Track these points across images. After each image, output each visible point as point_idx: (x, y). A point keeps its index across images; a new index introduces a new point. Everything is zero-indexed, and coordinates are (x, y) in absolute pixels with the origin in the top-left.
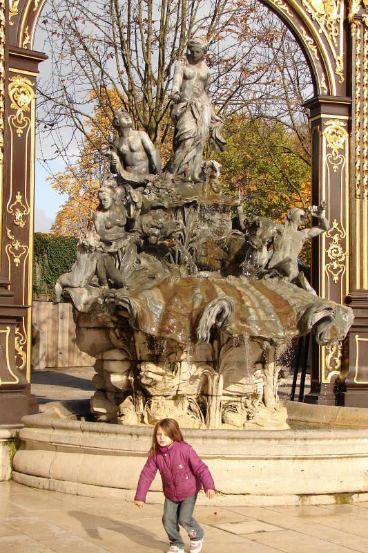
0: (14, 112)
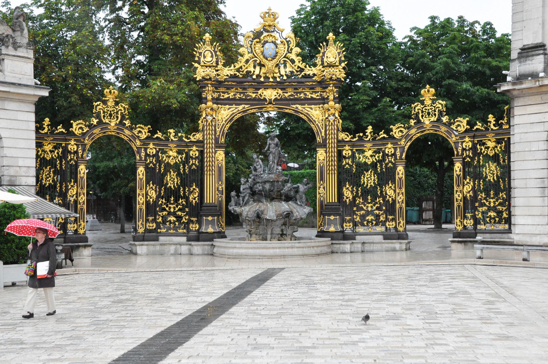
0: (218, 160)
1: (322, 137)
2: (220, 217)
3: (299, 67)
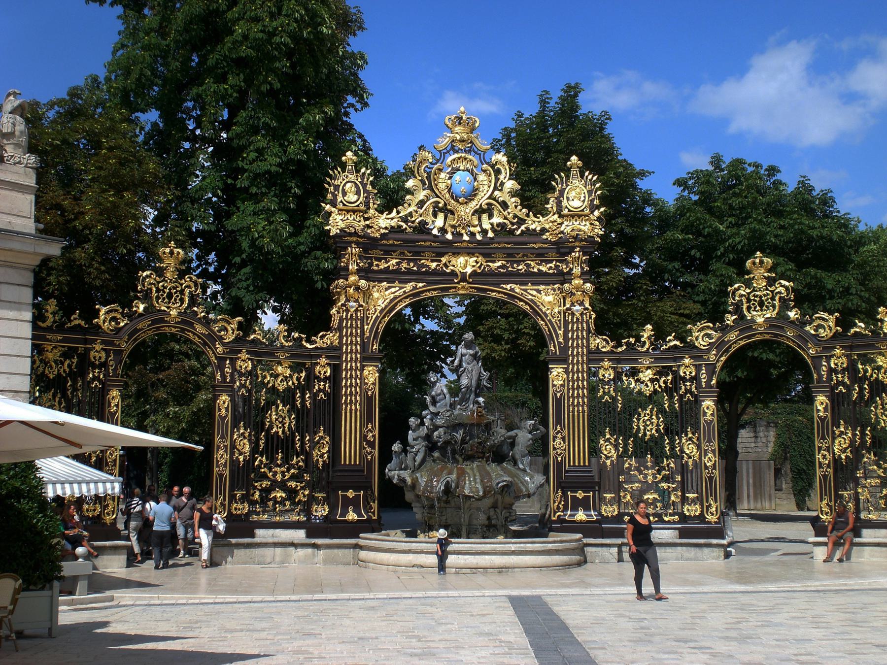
1: (559, 343)
2: (369, 492)
3: (515, 216)
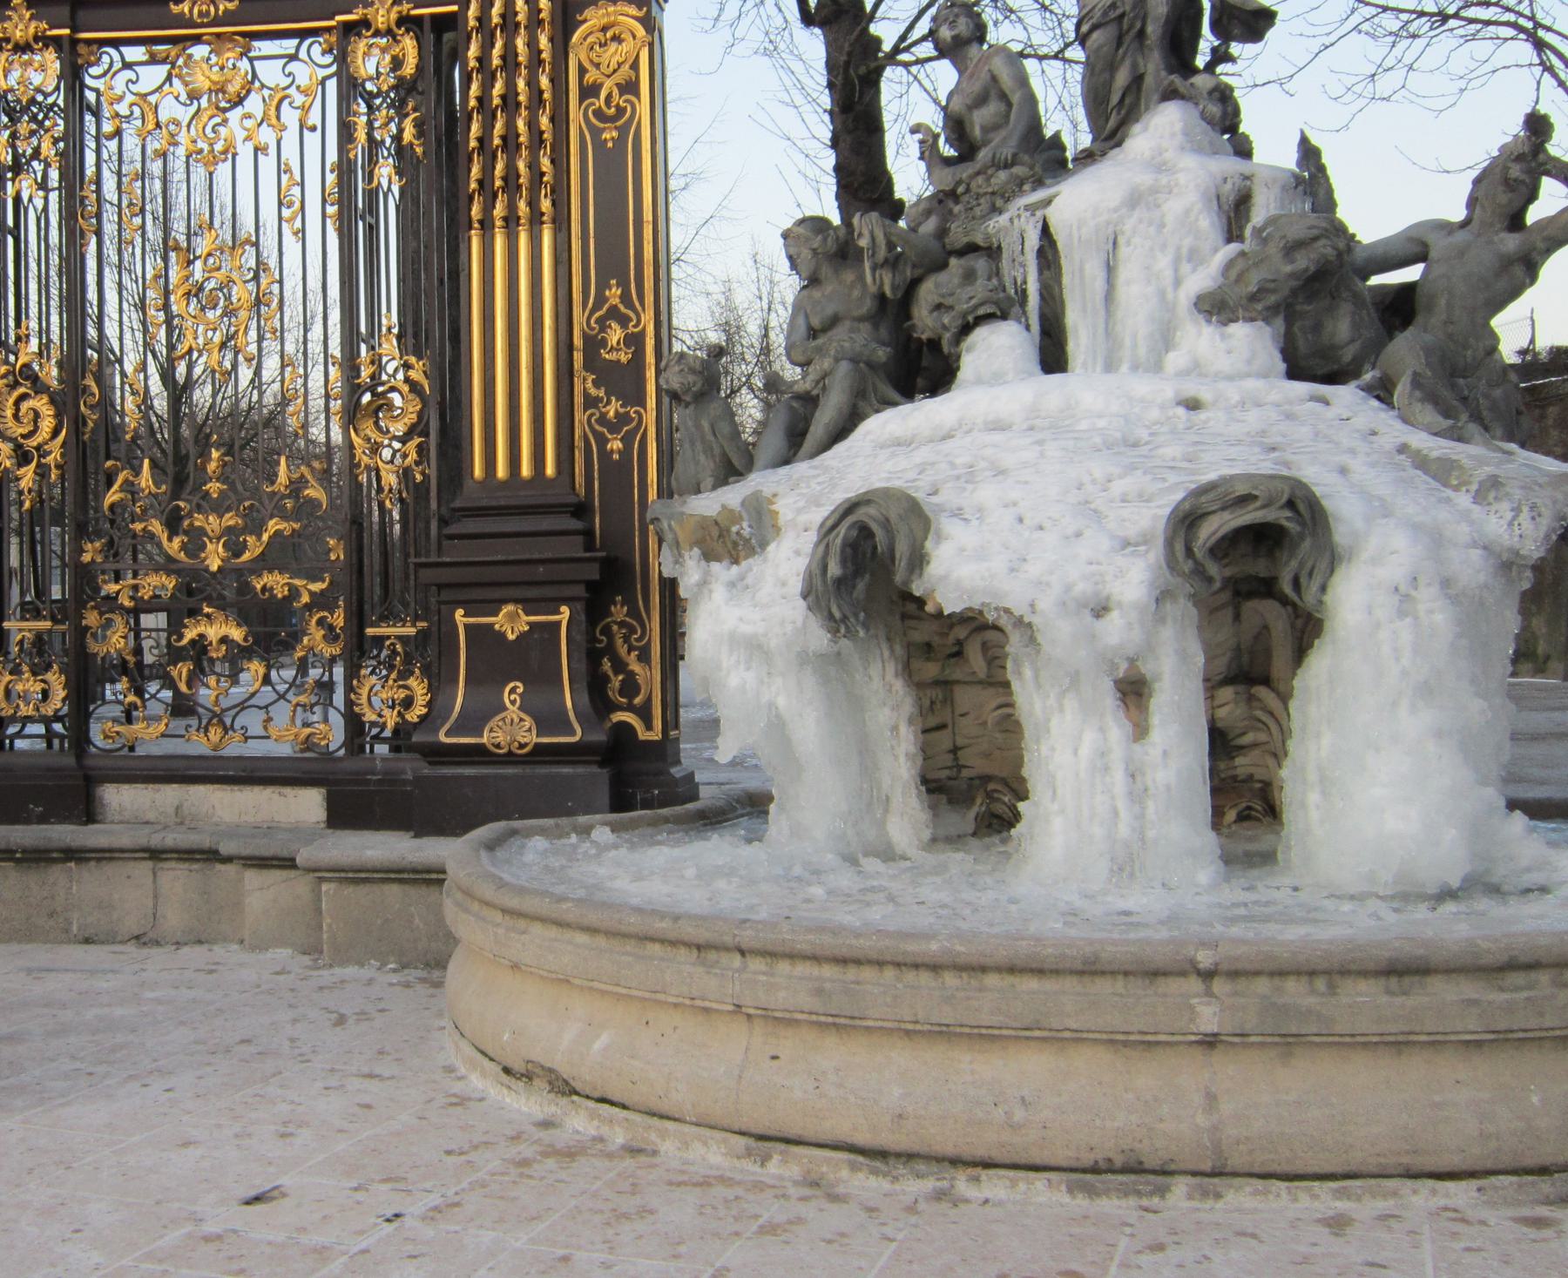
2: (619, 612)
